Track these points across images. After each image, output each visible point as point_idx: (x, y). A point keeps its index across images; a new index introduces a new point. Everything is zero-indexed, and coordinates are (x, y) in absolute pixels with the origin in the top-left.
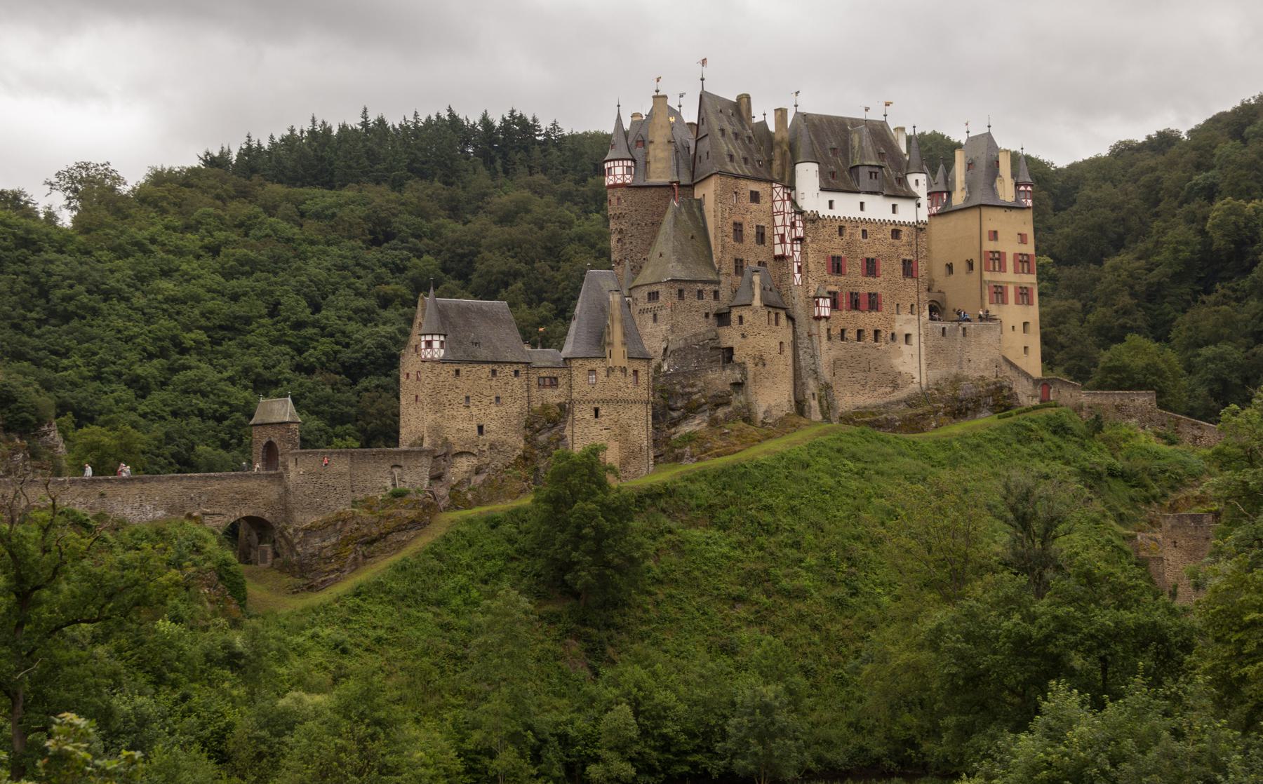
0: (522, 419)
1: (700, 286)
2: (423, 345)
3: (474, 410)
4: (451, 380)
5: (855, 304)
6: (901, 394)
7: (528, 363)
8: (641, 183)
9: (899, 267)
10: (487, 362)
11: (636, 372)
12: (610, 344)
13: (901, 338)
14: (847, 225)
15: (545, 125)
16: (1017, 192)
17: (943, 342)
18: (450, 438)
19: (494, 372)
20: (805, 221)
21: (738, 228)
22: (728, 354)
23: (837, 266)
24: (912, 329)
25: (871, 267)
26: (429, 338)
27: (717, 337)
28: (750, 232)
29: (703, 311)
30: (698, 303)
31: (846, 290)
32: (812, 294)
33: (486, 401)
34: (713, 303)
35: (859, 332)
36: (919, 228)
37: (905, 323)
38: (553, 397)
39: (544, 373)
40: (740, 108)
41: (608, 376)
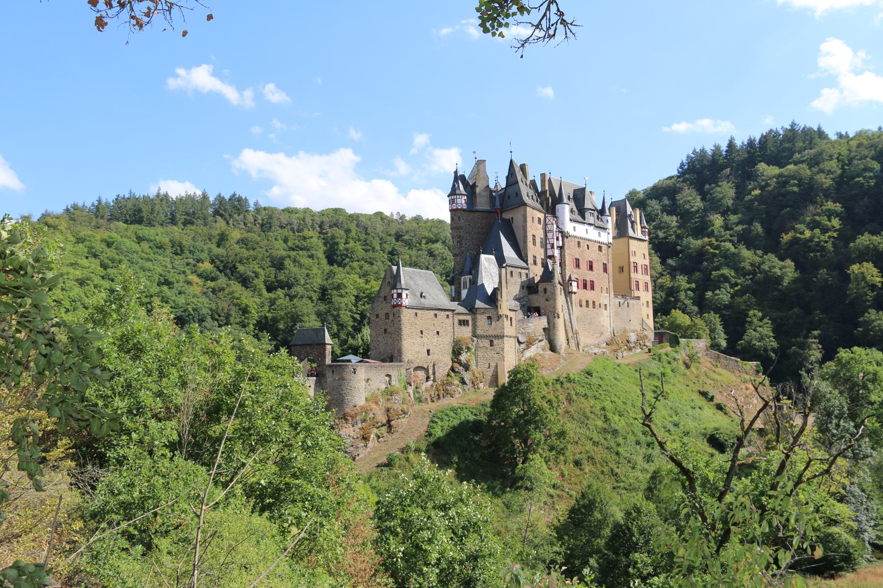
1: (520, 270)
2: (395, 296)
3: (425, 339)
4: (413, 319)
5: (585, 287)
7: (453, 311)
10: (432, 309)
11: (511, 318)
13: (603, 306)
14: (581, 241)
15: (251, 203)
16: (642, 231)
19: (436, 315)
24: (606, 302)
26: (399, 291)
27: (529, 301)
28: (538, 240)
31: (581, 278)
32: (567, 278)
35: (587, 302)
36: (609, 245)
37: (605, 298)
39: (462, 318)
41: (498, 320)
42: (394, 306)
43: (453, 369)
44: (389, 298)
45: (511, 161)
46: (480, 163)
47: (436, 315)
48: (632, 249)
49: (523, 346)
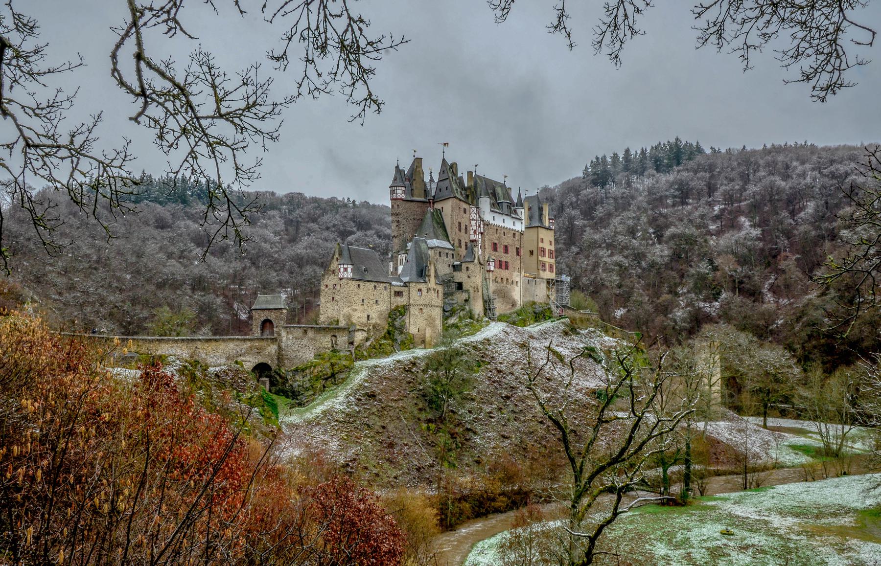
0: (387, 312)
2: (342, 270)
4: (356, 290)
5: (501, 267)
6: (515, 309)
8: (409, 199)
9: (515, 250)
12: (429, 276)
17: (528, 286)
18: (354, 321)
19: (375, 287)
20: (484, 225)
21: (460, 223)
22: (460, 286)
23: (495, 247)
24: (518, 279)
25: (506, 250)
28: (463, 227)
29: (448, 263)
30: (446, 259)
32: (486, 259)
33: (371, 302)
34: (452, 260)
38: (401, 301)
39: (397, 289)
40: (454, 167)
42: (341, 279)
43: (389, 332)
44: (337, 271)
45: (444, 160)
46: (418, 162)
47: (375, 287)
48: (541, 236)
49: (447, 314)
